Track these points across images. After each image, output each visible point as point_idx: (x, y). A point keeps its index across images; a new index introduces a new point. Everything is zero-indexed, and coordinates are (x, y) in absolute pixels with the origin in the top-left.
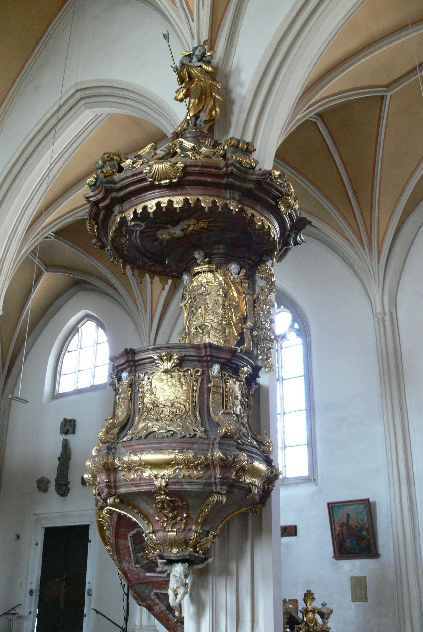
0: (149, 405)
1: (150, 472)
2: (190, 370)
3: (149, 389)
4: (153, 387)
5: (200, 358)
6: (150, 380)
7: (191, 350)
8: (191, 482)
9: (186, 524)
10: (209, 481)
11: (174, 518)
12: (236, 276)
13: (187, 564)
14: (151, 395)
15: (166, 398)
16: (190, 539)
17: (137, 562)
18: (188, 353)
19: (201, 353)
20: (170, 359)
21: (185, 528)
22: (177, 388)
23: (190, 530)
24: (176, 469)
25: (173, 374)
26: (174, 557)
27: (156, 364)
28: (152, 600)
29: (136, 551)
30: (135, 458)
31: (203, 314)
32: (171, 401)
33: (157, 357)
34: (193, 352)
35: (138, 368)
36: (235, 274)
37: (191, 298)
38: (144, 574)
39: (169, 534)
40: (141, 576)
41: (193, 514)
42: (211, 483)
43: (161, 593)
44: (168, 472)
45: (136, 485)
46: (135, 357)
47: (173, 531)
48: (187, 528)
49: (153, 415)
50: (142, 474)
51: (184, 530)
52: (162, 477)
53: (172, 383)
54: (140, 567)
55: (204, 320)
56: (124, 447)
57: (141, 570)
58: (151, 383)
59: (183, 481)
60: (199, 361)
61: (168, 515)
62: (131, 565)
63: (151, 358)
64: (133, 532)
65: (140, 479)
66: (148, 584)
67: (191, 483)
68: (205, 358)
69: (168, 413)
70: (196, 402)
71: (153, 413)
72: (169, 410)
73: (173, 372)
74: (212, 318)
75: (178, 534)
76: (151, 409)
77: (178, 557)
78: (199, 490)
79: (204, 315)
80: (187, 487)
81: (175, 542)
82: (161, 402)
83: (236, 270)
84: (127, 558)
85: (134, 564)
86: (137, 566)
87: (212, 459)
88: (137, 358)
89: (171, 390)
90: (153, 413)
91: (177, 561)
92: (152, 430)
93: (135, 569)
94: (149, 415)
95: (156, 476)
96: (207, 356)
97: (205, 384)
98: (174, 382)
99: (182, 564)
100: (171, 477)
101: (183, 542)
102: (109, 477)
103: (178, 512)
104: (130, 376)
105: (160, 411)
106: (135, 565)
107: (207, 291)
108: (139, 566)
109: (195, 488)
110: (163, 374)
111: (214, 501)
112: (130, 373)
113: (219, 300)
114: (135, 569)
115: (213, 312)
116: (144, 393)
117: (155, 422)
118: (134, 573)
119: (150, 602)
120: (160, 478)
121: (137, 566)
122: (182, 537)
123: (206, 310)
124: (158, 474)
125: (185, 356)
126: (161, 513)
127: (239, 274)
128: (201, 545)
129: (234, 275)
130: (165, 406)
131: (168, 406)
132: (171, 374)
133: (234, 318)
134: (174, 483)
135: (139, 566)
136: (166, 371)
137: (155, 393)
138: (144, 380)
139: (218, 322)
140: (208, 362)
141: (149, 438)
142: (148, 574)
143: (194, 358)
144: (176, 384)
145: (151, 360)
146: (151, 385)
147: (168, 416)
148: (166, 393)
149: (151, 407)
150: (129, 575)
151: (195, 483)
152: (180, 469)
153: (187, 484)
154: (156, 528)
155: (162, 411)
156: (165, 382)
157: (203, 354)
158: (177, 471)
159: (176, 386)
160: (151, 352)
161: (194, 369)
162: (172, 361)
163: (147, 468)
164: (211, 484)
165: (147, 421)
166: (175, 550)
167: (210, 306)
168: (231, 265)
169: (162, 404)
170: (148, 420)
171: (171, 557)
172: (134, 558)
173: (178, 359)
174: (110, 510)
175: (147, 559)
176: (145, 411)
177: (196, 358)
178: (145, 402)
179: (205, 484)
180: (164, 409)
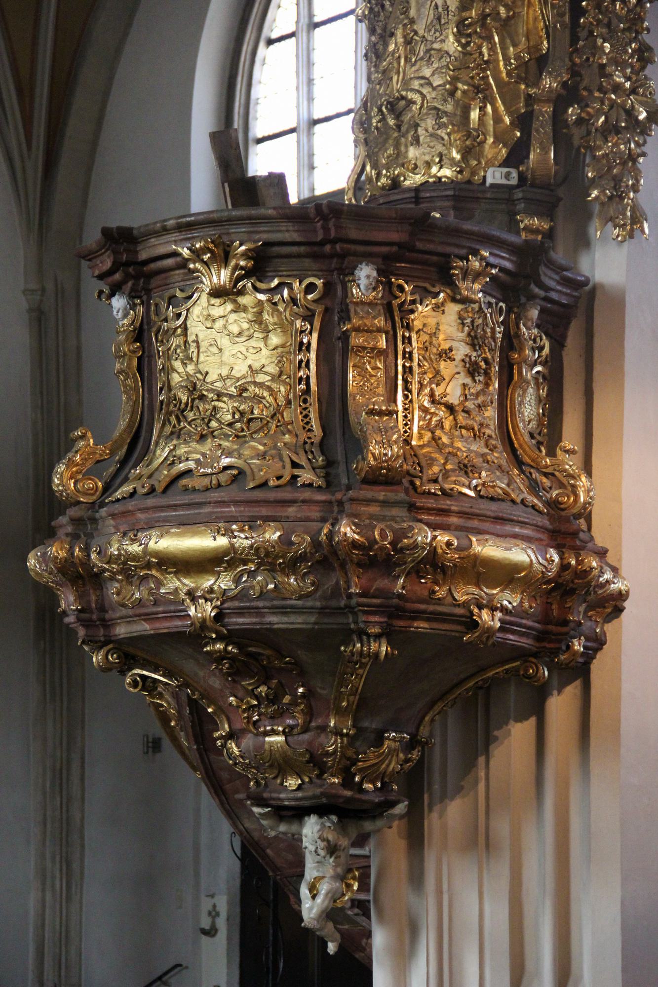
1: (178, 583)
8: (283, 607)
11: (274, 699)
19: (315, 231)
45: (148, 617)
59: (260, 604)
60: (315, 256)
67: (283, 610)
68: (328, 248)
75: (290, 739)
80: (276, 620)
95: (191, 594)
101: (308, 762)
103: (280, 682)
109: (296, 621)
124: (196, 589)
140: (342, 256)
143: (294, 249)
153: (274, 613)
154: (238, 726)
157: (320, 236)
166: (292, 783)
177: (302, 249)
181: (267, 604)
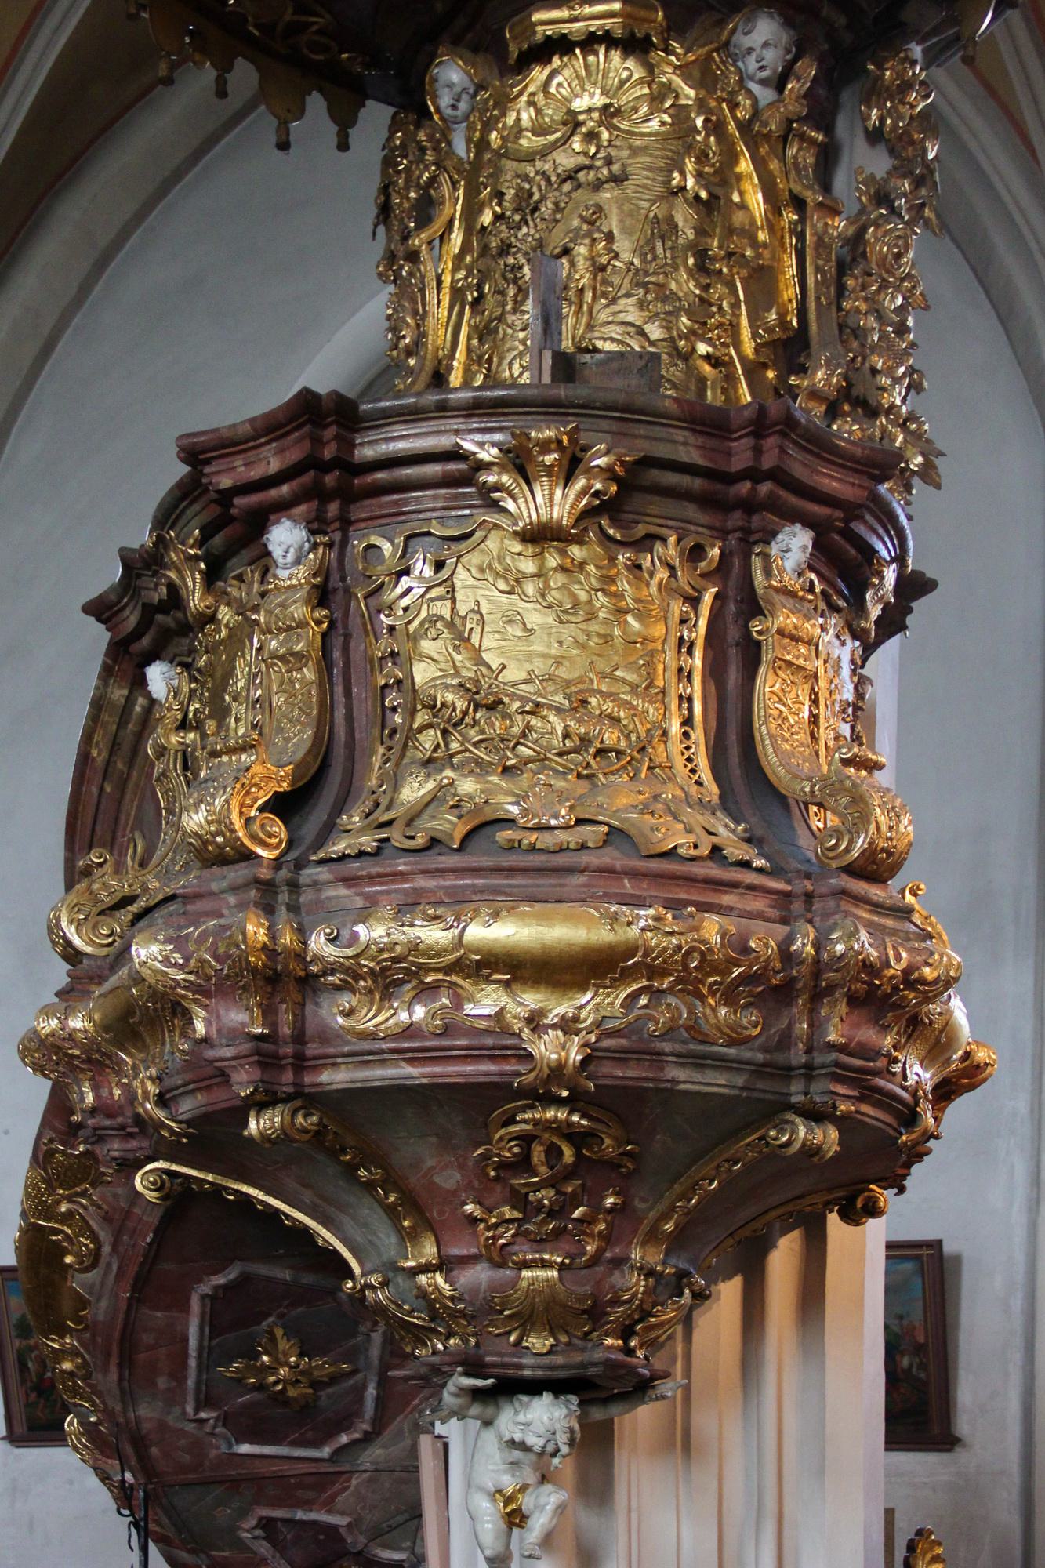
0: (450, 697)
2: (664, 540)
3: (441, 618)
4: (462, 609)
5: (719, 487)
6: (444, 574)
7: (680, 435)
8: (704, 1057)
9: (607, 1239)
10: (780, 1058)
11: (558, 1211)
12: (765, 95)
13: (574, 1399)
14: (456, 648)
15: (540, 667)
16: (616, 1302)
17: (205, 1401)
18: (662, 451)
20: (572, 466)
21: (600, 1251)
22: (594, 627)
23: (620, 1262)
24: (634, 997)
25: (576, 551)
26: (532, 1368)
27: (486, 490)
28: (240, 1545)
29: (210, 1357)
30: (433, 935)
31: (581, 291)
32: (569, 683)
33: (495, 451)
34: (687, 449)
35: (358, 511)
36: (763, 82)
37: (499, 195)
38: (230, 1446)
39: (525, 1273)
40: (213, 1453)
41: (643, 1200)
42: (790, 1068)
43: (286, 1521)
44: (586, 1003)
45: (416, 1057)
46: (353, 446)
47: (545, 1264)
48: (608, 1255)
49: (475, 744)
50: (458, 1005)
51: (595, 1260)
52: (568, 1025)
53: (574, 596)
54: (217, 1419)
55: (590, 327)
56: (349, 881)
57: (219, 1430)
58: (454, 590)
59: (667, 1047)
60: (706, 501)
61: (531, 1197)
62: (177, 1410)
63: (455, 454)
64: (220, 1280)
65: (447, 1031)
66: (234, 1485)
67: (698, 1062)
68: (745, 487)
69: (557, 743)
70: (690, 700)
71: (474, 735)
72: (559, 729)
73: (579, 541)
74: (633, 316)
75: (568, 1275)
76: (465, 713)
77: (552, 1368)
78: (736, 1092)
79: (588, 296)
80: (684, 1078)
81: (547, 1309)
82: (516, 684)
83: (774, 58)
84: (162, 1382)
85: (190, 1409)
86: (203, 1415)
87: (817, 961)
88: (367, 453)
89: (568, 632)
90: (474, 735)
91: (534, 1388)
92: (489, 813)
93: (190, 1427)
94: (455, 746)
95: (535, 1021)
96: (754, 474)
97: (730, 619)
98: (583, 596)
99: (556, 1397)
100: (612, 1024)
101: (584, 1312)
102: (269, 1013)
103: (583, 1186)
104: (314, 547)
105: (516, 730)
106: (197, 1410)
107: (609, 161)
108: (214, 1414)
109: (717, 1082)
110: (517, 547)
111: (788, 1144)
112: (313, 532)
113: (679, 219)
114: (190, 1427)
115: (645, 285)
116: (414, 638)
117: (495, 779)
118: (182, 1442)
119: (226, 1554)
120: (554, 1027)
121: (203, 1415)
122: (587, 1289)
123: (603, 269)
124: (542, 1013)
125: (647, 462)
126: (498, 1188)
127: (780, 87)
128: (653, 1327)
129: (754, 87)
130: (538, 705)
131: (559, 710)
132: (563, 553)
133: (746, 332)
134: (621, 1056)
135: (214, 1414)
136: (538, 536)
137: (475, 640)
138: (406, 572)
139: (672, 340)
140: (749, 506)
141: (472, 845)
142: (245, 1448)
144: (590, 602)
145: (452, 467)
146: (454, 601)
147: (560, 754)
148: (538, 648)
149: (460, 705)
150: (154, 1451)
151: (722, 1063)
152: (656, 994)
153: (682, 1064)
155: (528, 727)
156: (530, 588)
157: (738, 464)
158: (643, 1001)
159: (591, 616)
160: (454, 424)
161: (679, 541)
162: (580, 483)
163: (488, 980)
164: (785, 1072)
165: (448, 773)
166: (538, 1342)
167: (624, 246)
168: (750, 19)
169: (524, 700)
170: (453, 767)
171: (520, 1367)
172: (198, 1382)
173: (609, 473)
174: (172, 1174)
175: (261, 1387)
176: (430, 726)
177: (697, 483)
178: (419, 679)
179: (761, 1071)
180: (534, 721)
181: (678, 1047)
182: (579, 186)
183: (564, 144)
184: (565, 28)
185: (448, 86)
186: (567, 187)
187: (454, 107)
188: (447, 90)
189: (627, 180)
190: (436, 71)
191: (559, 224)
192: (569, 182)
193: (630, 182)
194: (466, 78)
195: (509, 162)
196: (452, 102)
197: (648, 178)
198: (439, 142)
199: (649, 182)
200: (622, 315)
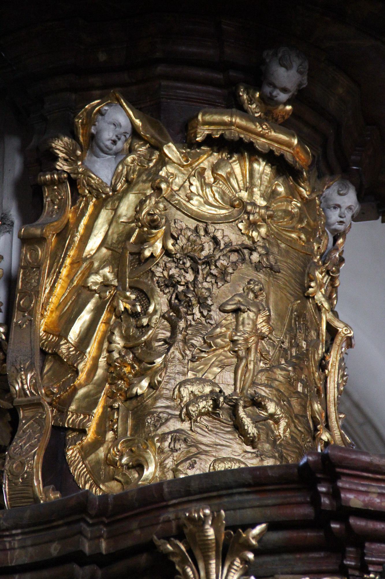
182: (243, 260)
183: (232, 222)
184: (253, 138)
185: (114, 124)
186: (234, 257)
187: (114, 142)
188: (112, 126)
189: (279, 272)
190: (106, 108)
191: (226, 285)
192: (236, 254)
193: (280, 274)
194: (130, 126)
195: (179, 212)
196: (114, 138)
197: (292, 277)
198: (78, 158)
199: (293, 281)
200: (277, 383)
